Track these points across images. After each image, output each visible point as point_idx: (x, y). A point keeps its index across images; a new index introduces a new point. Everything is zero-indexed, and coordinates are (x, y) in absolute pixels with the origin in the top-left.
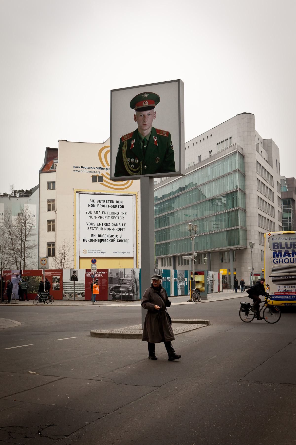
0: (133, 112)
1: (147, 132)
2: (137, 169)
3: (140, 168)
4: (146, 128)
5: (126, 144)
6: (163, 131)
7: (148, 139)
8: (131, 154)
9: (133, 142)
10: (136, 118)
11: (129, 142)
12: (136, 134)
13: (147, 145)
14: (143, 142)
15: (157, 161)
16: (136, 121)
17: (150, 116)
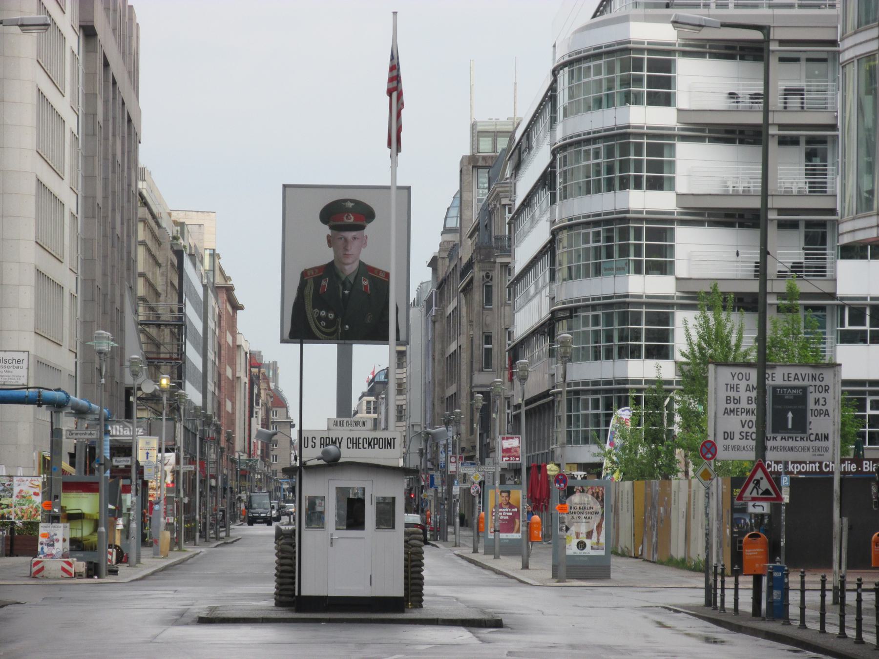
0: (326, 230)
1: (350, 269)
2: (332, 330)
3: (337, 329)
4: (350, 260)
5: (311, 285)
6: (379, 271)
7: (352, 280)
8: (320, 301)
9: (325, 283)
10: (330, 241)
11: (317, 281)
12: (330, 269)
13: (351, 290)
14: (344, 284)
15: (369, 319)
16: (330, 246)
17: (356, 243)
